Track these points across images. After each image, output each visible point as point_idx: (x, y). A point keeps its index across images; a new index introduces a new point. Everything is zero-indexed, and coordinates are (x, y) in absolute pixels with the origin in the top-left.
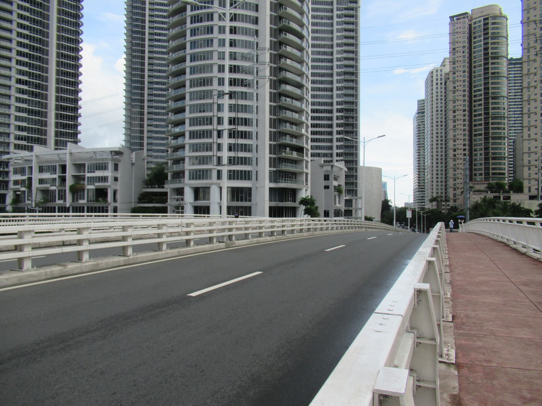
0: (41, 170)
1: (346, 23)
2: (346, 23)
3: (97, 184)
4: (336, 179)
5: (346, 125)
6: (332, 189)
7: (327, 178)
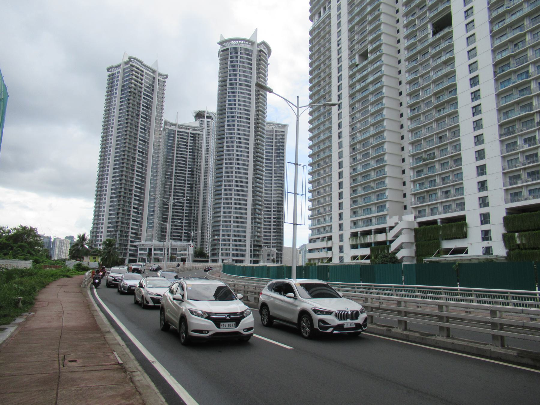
0: (155, 250)
1: (278, 180)
2: (278, 180)
3: (182, 257)
4: (272, 256)
5: (277, 229)
6: (271, 260)
7: (268, 255)
